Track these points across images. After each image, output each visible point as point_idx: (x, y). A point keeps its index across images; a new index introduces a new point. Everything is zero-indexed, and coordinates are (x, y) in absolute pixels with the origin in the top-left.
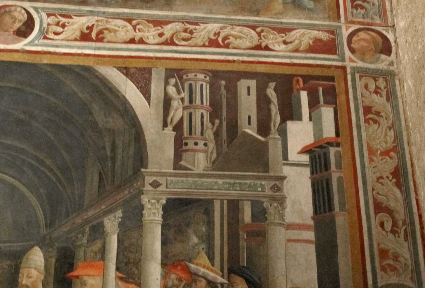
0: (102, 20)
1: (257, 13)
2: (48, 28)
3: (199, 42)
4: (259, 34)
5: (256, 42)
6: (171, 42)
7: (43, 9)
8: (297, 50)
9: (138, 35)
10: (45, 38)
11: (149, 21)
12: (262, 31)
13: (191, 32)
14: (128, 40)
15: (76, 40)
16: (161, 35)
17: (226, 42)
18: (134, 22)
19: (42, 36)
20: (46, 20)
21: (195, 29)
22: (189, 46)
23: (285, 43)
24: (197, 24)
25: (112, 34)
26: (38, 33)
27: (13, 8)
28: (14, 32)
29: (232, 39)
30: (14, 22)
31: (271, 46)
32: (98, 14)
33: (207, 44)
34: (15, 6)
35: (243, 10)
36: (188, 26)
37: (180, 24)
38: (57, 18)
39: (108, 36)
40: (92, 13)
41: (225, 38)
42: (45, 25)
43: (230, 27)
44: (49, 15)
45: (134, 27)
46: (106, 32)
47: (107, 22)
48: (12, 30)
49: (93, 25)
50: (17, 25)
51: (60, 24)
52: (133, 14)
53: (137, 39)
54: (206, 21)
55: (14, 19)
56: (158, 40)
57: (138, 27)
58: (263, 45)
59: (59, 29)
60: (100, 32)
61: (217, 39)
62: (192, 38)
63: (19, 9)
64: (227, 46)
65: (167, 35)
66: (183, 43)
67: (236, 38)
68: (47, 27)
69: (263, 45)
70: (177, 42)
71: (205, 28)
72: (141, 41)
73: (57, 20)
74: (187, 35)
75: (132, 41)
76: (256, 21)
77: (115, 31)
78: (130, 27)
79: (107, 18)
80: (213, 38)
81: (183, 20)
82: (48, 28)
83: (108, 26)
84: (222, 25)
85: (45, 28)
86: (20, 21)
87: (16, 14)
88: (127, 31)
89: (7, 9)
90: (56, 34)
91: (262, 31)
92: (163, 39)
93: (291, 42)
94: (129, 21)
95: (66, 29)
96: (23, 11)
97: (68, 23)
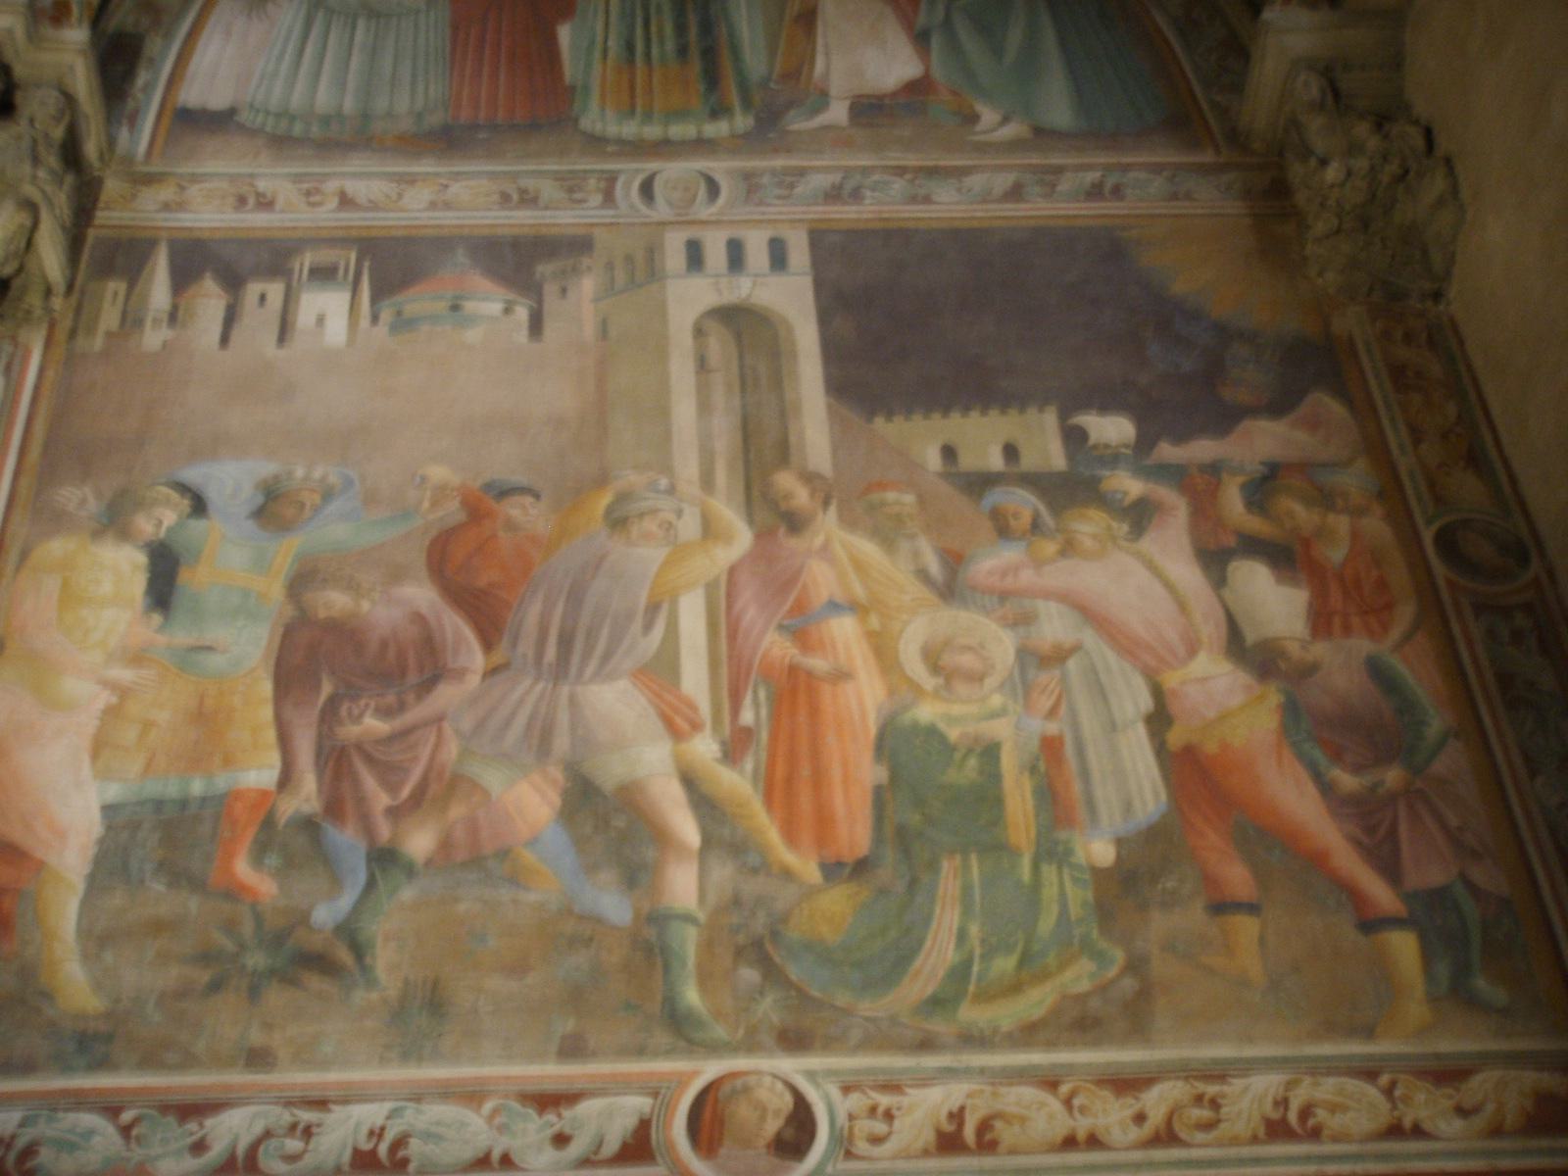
0: (982, 1091)
1: (1369, 1033)
2: (851, 1129)
3: (1241, 1128)
4: (1389, 1092)
5: (1384, 1115)
6: (1166, 1136)
7: (830, 1073)
8: (1496, 1131)
9: (1082, 1126)
10: (849, 1155)
11: (1101, 1082)
12: (1393, 1084)
13: (1215, 1104)
14: (1059, 1139)
15: (926, 1153)
16: (1140, 1118)
17: (1311, 1122)
18: (1065, 1089)
19: (840, 1148)
20: (846, 1104)
21: (1224, 1096)
22: (1219, 1144)
23: (1462, 1112)
24: (1222, 1078)
25: (1016, 1128)
26: (829, 1143)
27: (752, 1080)
28: (768, 1146)
29: (1321, 1114)
30: (763, 1118)
31: (1427, 1126)
32: (966, 1073)
33: (1261, 1132)
34: (759, 1073)
35: (1330, 1029)
36: (1201, 1087)
37: (1180, 1084)
38: (869, 1098)
39: (1005, 1133)
40: (949, 1073)
41: (1306, 1113)
42: (842, 1119)
43: (1307, 1080)
44: (847, 1090)
45: (1068, 1103)
46: (998, 1124)
47: (994, 1094)
48: (762, 1142)
49: (962, 1109)
50: (772, 1126)
51: (880, 1110)
52: (1054, 1066)
53: (1081, 1135)
54: (1247, 1067)
55: (762, 1110)
56: (1135, 1133)
57: (1076, 1102)
58: (1407, 1123)
59: (880, 1127)
60: (984, 1127)
61: (1284, 1120)
62: (1219, 1121)
63: (768, 1080)
64: (1315, 1134)
65: (1156, 1117)
66: (1200, 1137)
67: (1334, 1108)
68: (847, 1125)
69: (1407, 1123)
70: (1183, 1135)
71: (1246, 1089)
72: (1094, 1142)
73: (870, 1102)
74: (1204, 1114)
75: (1070, 1143)
76: (1370, 1057)
77: (1023, 1120)
78: (1055, 1105)
79: (993, 1084)
80: (1275, 1115)
81: (1187, 1071)
82: (851, 1129)
83: (998, 1106)
84: (1293, 1076)
85: (842, 1129)
86: (777, 1113)
87: (762, 1094)
88: (1051, 1117)
89: (739, 1083)
90: (876, 1140)
91: (1393, 1084)
92: (1148, 1129)
93: (1476, 1110)
94: (1051, 1084)
95: (897, 1123)
96: (779, 1086)
97: (899, 1109)
